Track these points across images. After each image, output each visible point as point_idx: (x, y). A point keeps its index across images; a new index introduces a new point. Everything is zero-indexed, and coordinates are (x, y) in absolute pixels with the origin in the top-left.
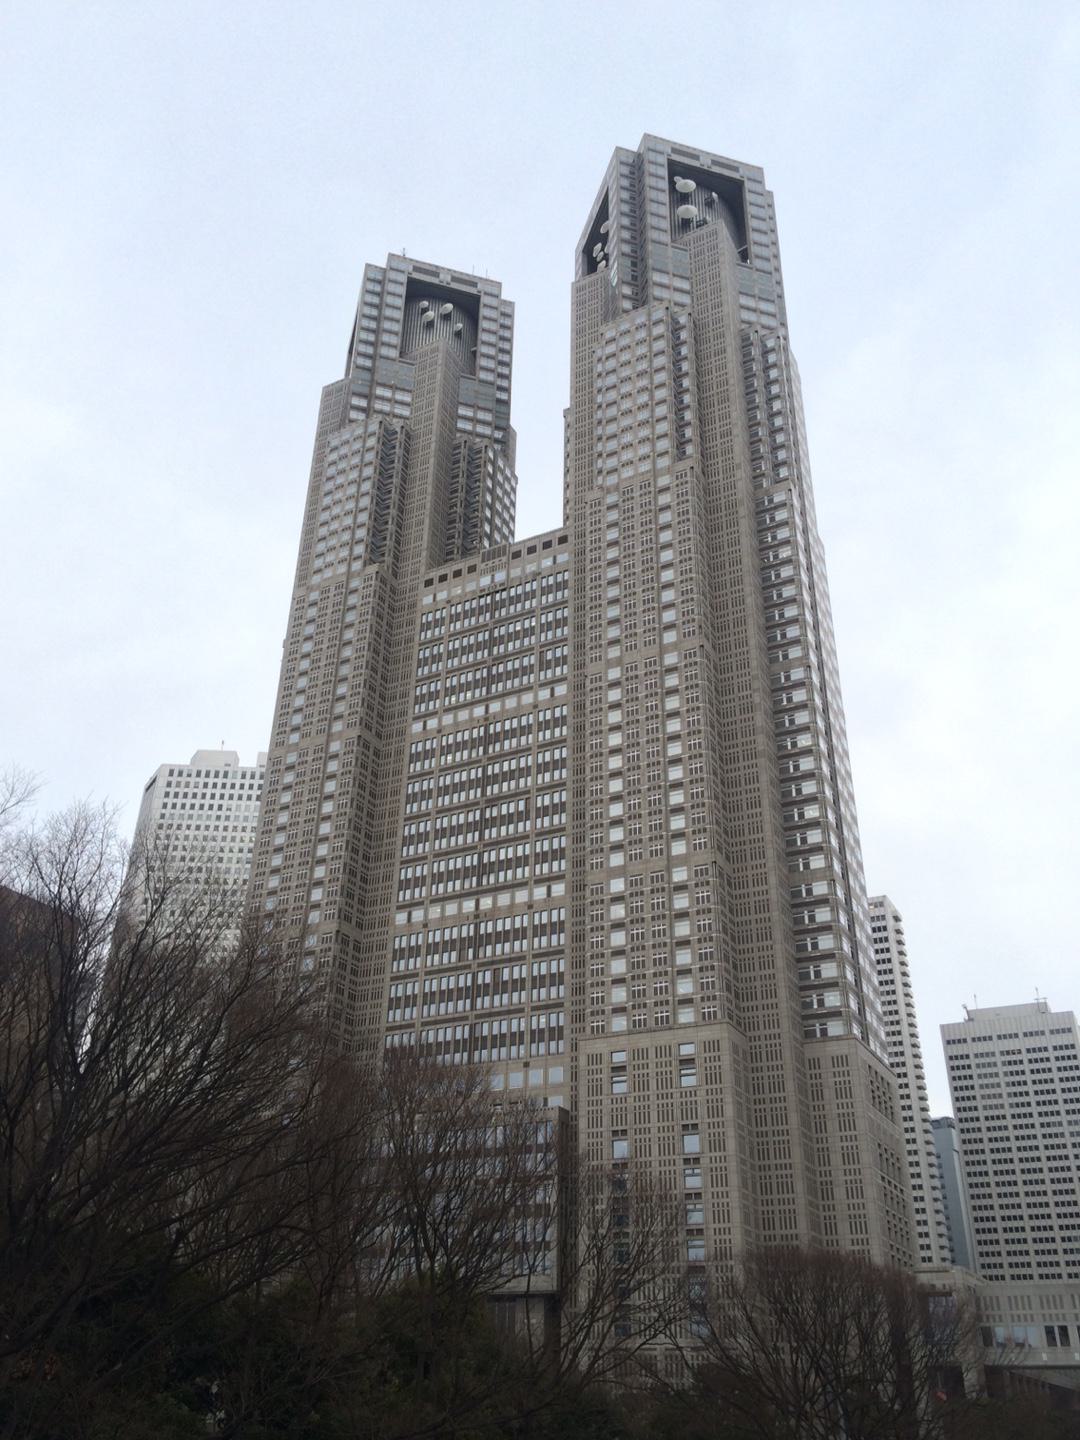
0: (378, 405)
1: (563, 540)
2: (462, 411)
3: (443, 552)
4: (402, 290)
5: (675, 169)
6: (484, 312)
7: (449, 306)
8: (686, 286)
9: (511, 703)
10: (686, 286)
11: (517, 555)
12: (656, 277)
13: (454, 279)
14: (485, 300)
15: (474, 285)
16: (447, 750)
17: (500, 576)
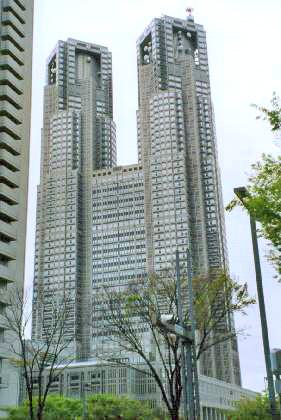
0: (70, 104)
1: (141, 168)
2: (99, 104)
3: (97, 167)
4: (73, 54)
5: (175, 30)
6: (103, 61)
7: (89, 58)
8: (179, 79)
9: (126, 223)
10: (179, 79)
11: (125, 171)
12: (171, 78)
13: (92, 47)
14: (103, 55)
15: (98, 49)
16: (105, 237)
17: (120, 178)
